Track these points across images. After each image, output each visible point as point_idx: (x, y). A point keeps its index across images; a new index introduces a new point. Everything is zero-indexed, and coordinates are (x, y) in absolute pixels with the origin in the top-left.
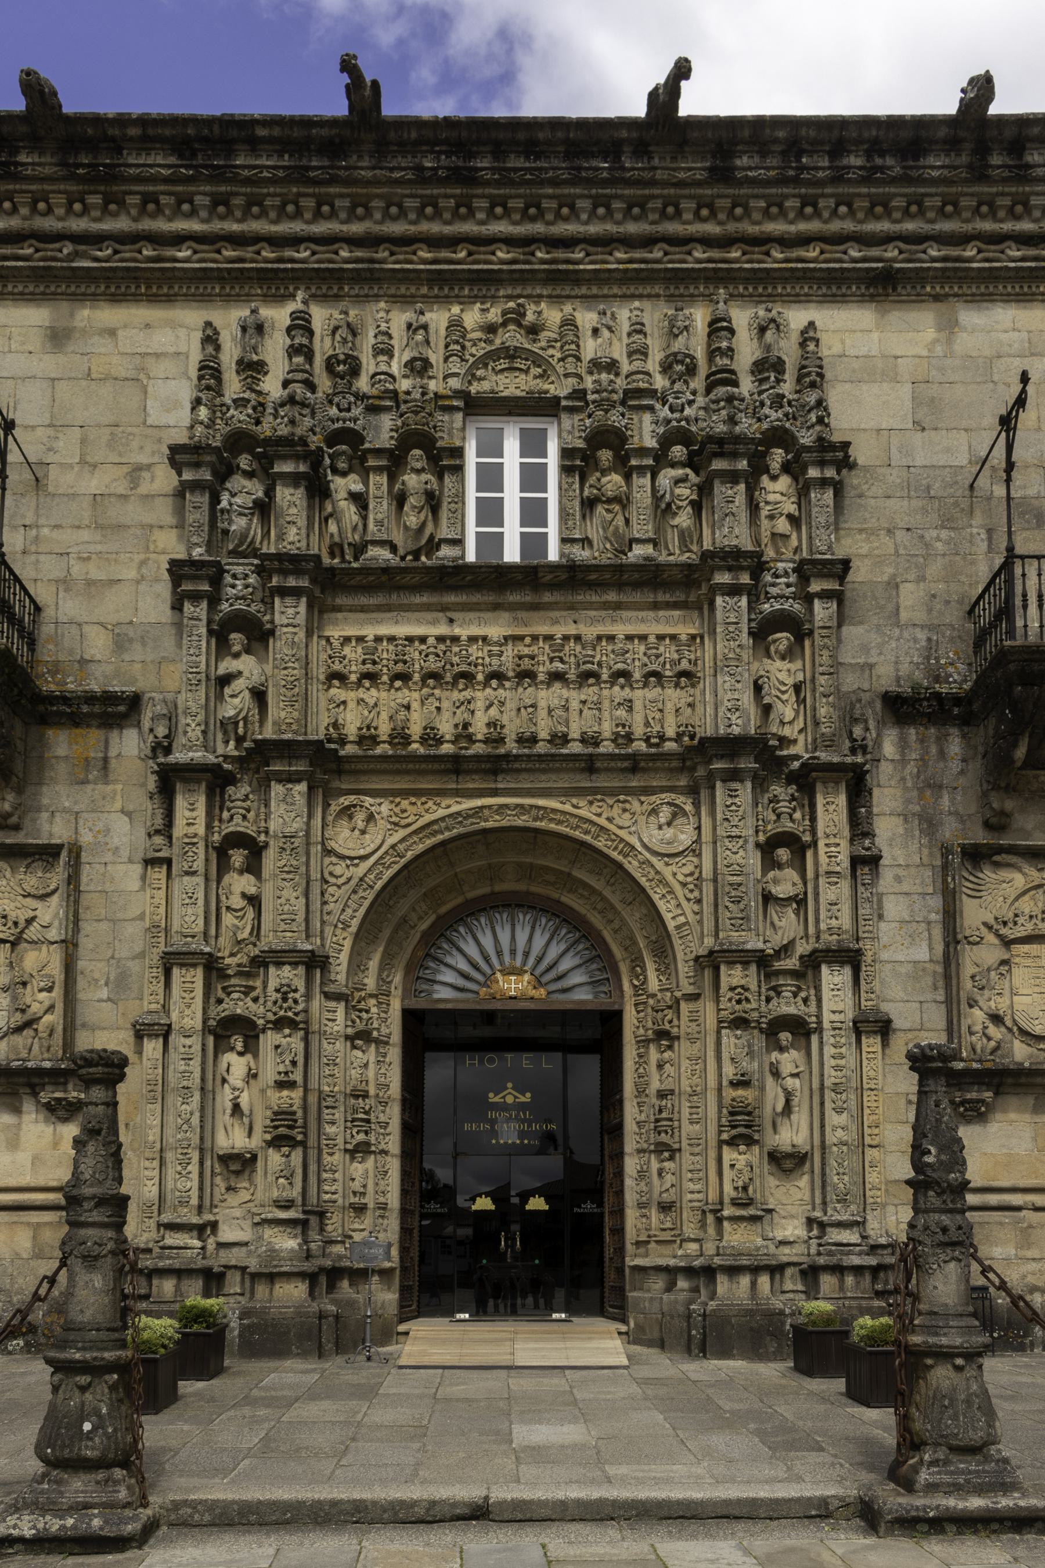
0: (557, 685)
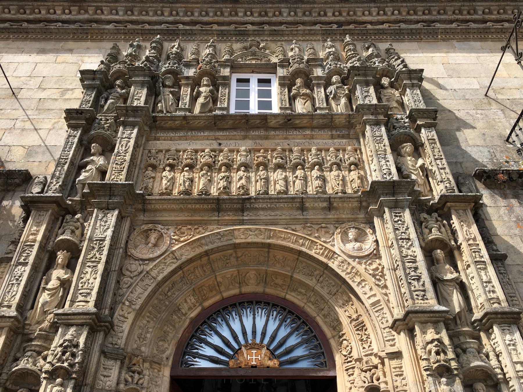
0: (279, 171)
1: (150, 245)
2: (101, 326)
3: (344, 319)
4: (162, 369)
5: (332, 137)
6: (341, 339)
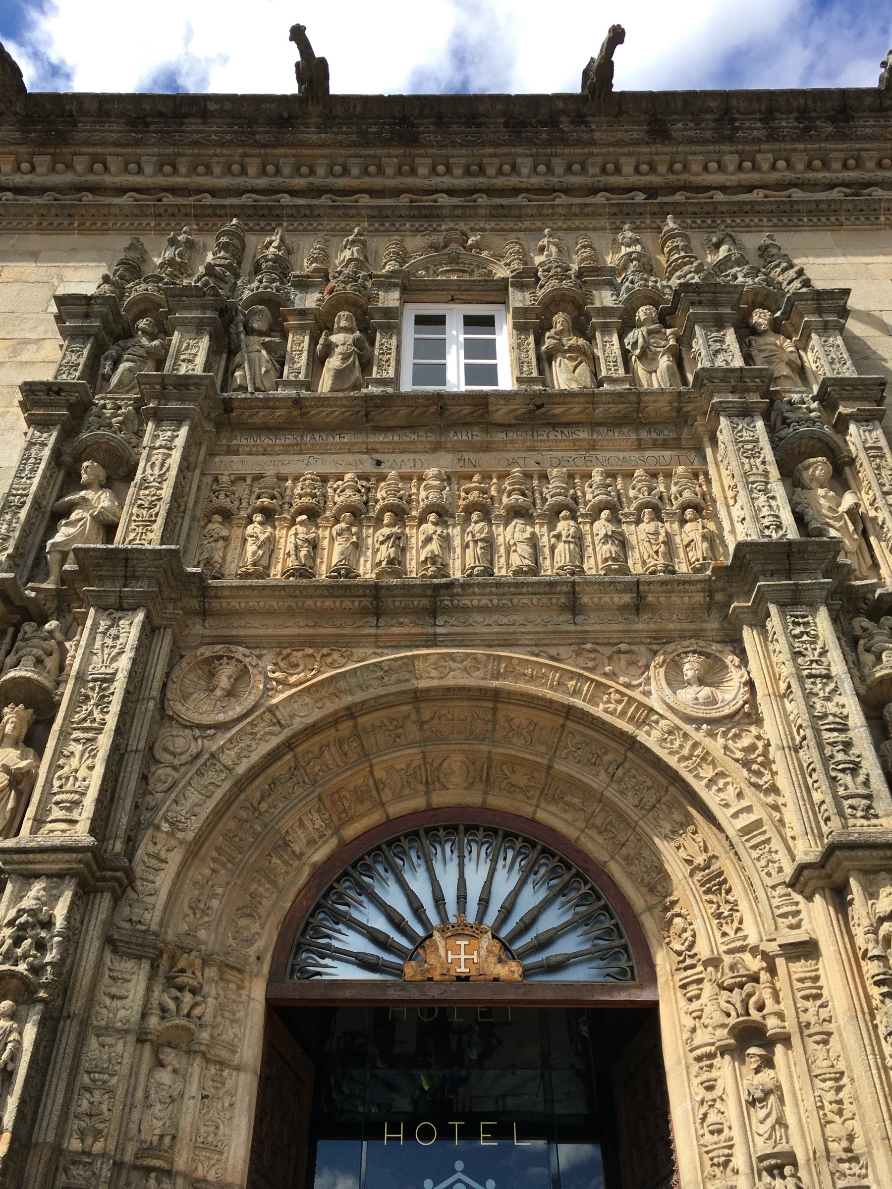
0: (518, 523)
1: (218, 692)
2: (105, 879)
3: (674, 866)
4: (247, 984)
5: (640, 446)
6: (669, 914)
